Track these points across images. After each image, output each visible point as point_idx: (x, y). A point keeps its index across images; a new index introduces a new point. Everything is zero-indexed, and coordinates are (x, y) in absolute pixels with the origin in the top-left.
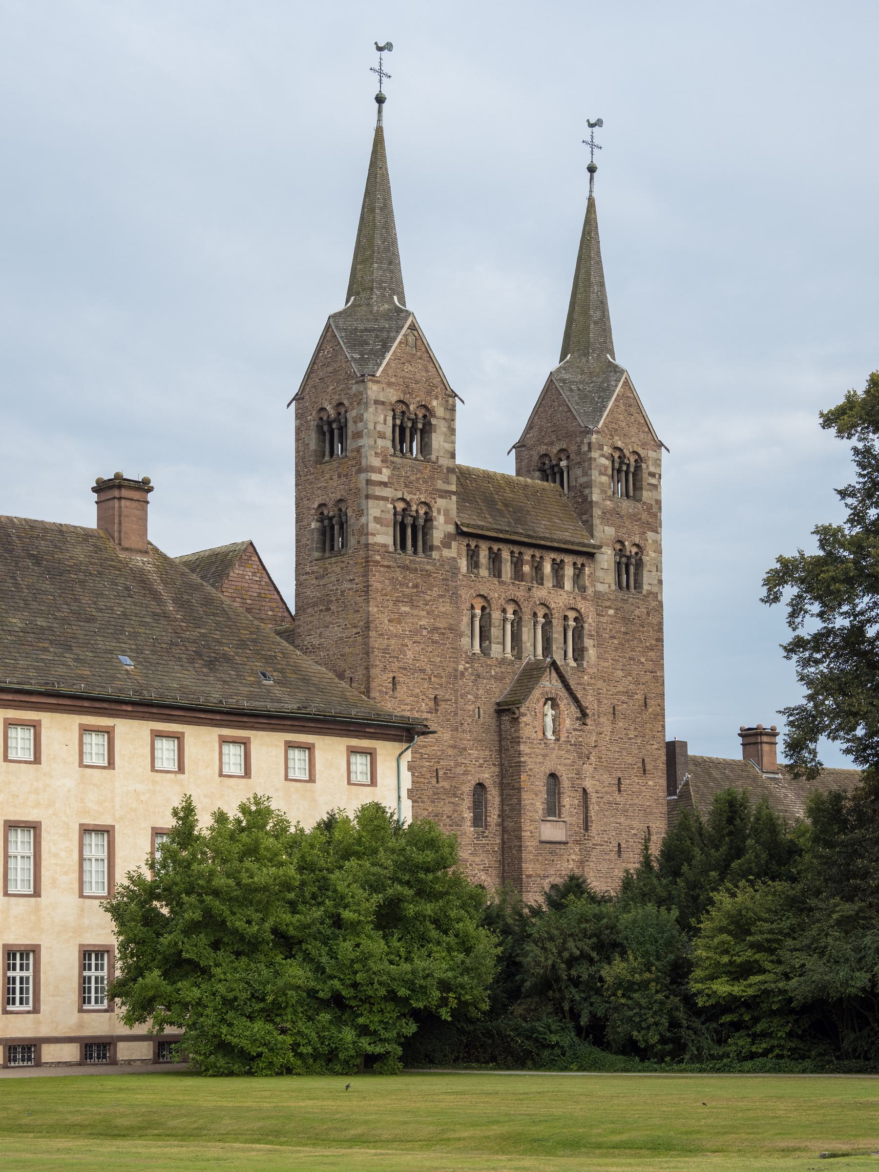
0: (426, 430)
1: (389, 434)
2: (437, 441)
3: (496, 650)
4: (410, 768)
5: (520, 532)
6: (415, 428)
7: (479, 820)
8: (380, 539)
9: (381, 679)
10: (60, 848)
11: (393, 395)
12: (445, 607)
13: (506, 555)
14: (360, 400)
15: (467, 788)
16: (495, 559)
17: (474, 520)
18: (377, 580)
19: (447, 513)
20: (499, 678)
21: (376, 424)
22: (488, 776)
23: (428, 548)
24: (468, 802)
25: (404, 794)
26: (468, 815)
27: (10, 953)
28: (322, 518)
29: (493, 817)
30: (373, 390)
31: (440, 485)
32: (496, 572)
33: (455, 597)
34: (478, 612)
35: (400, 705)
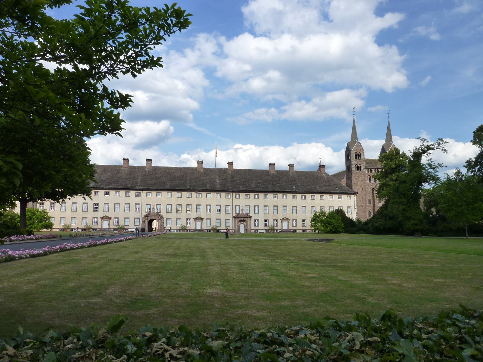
0: (360, 156)
1: (354, 156)
2: (362, 157)
3: (372, 182)
4: (356, 198)
5: (375, 166)
6: (358, 156)
7: (369, 203)
8: (353, 170)
9: (354, 187)
10: (308, 208)
11: (355, 152)
12: (363, 177)
13: (373, 170)
14: (351, 153)
15: (367, 199)
16: (371, 171)
17: (367, 166)
18: (353, 175)
19: (363, 166)
20: (372, 185)
21: (353, 156)
22: (371, 198)
23: (361, 170)
24: (368, 201)
25: (355, 201)
26: (368, 203)
27: (303, 220)
28: (348, 167)
29: (372, 203)
30: (352, 152)
31: (362, 162)
32: (372, 172)
33: (365, 176)
34: (369, 177)
35: (355, 190)
